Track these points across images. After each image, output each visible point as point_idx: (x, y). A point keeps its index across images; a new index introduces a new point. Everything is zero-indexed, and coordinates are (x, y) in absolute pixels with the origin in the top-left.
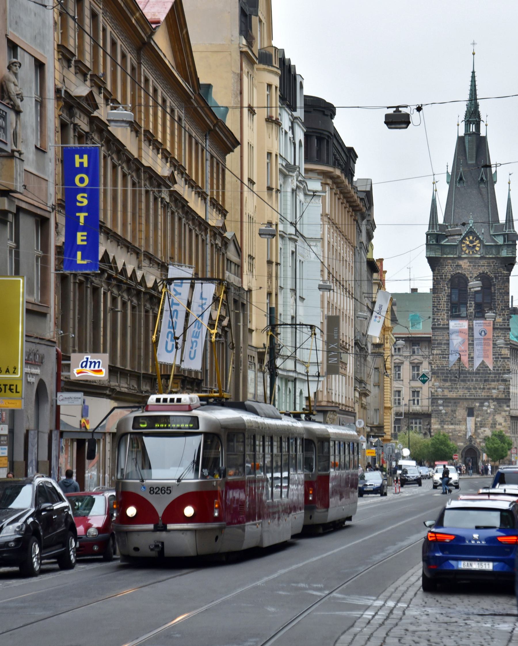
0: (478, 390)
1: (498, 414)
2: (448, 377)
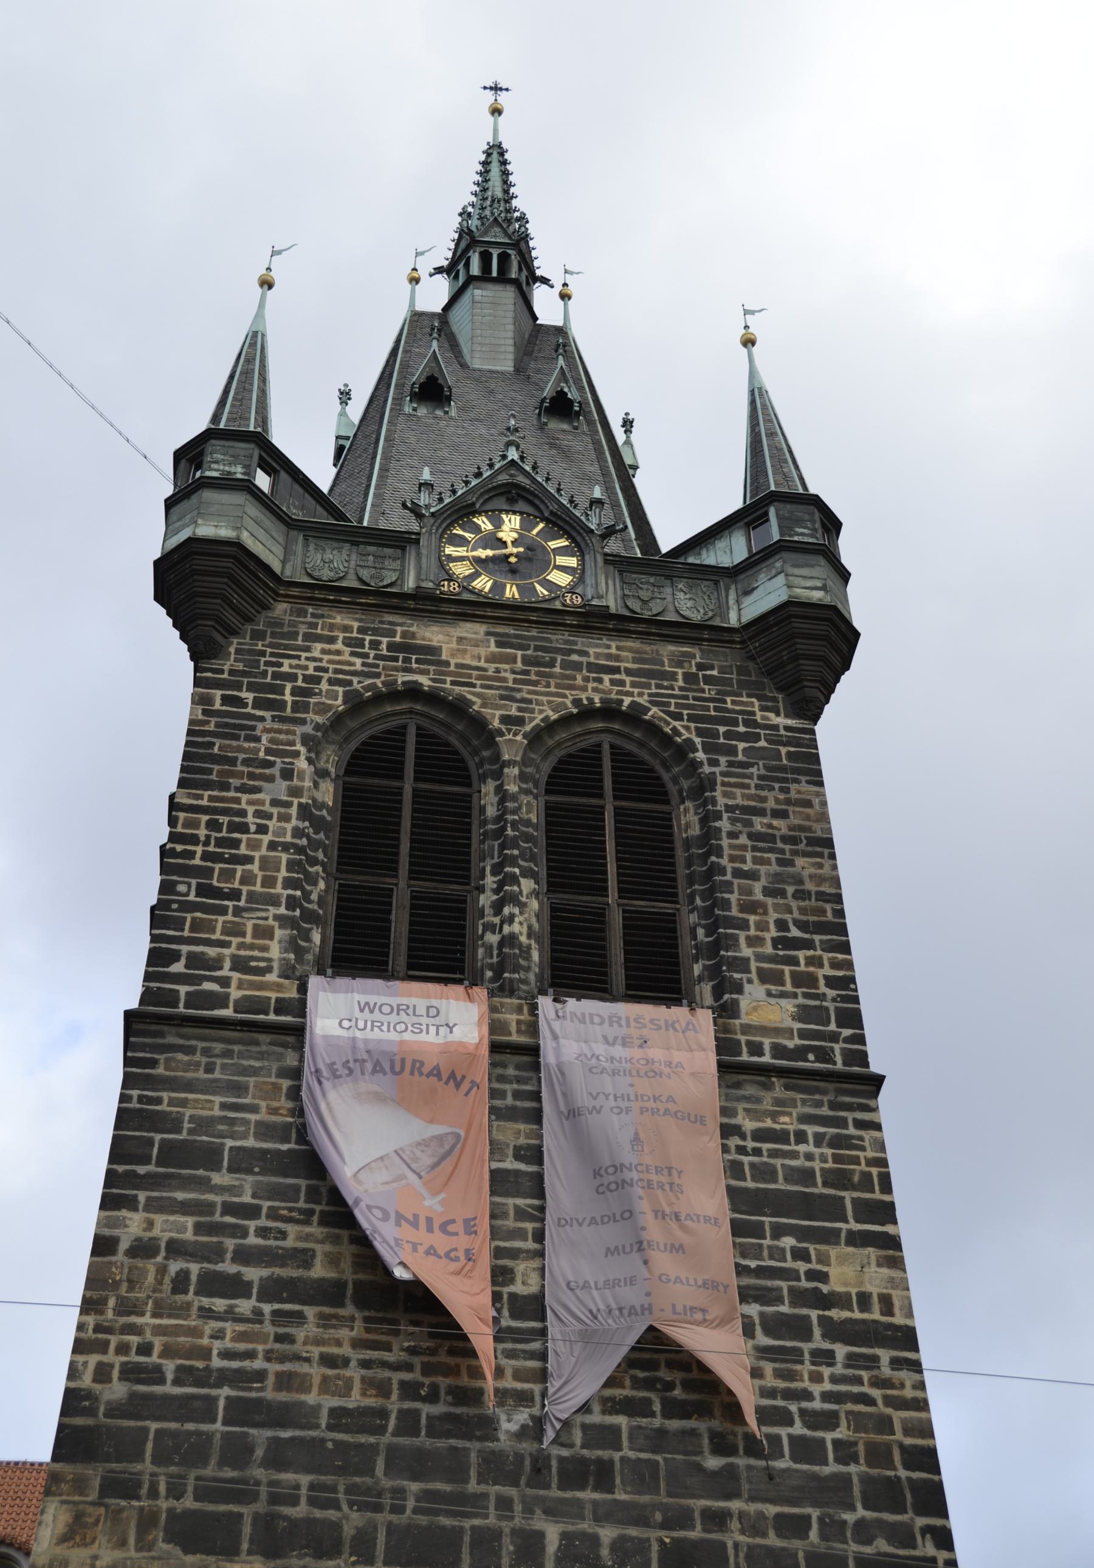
2: (243, 1494)
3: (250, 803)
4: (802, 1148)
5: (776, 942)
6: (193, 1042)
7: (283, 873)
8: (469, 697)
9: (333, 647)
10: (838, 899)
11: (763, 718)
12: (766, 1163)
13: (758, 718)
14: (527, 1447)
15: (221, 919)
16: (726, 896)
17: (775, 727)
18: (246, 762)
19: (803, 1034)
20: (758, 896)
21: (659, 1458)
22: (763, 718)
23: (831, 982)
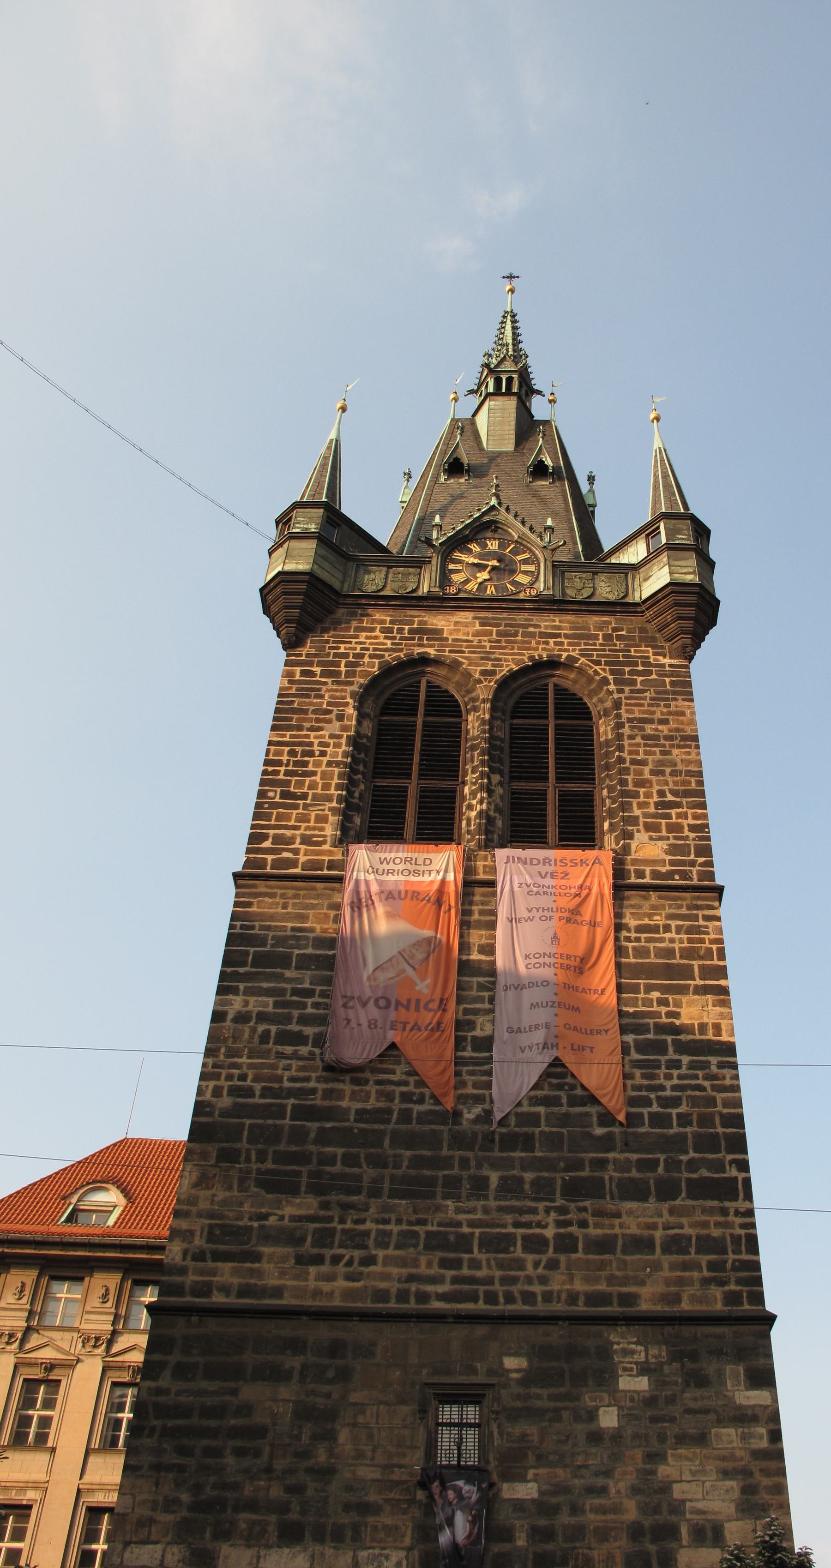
0: (518, 1251)
1: (682, 1439)
3: (316, 737)
4: (667, 935)
5: (657, 805)
6: (276, 890)
7: (336, 781)
8: (461, 659)
9: (373, 634)
10: (700, 774)
11: (655, 660)
12: (643, 946)
13: (651, 660)
14: (478, 1128)
15: (295, 812)
16: (626, 777)
17: (663, 666)
18: (315, 712)
19: (672, 863)
20: (647, 775)
21: (564, 1130)
22: (655, 660)
23: (692, 828)
